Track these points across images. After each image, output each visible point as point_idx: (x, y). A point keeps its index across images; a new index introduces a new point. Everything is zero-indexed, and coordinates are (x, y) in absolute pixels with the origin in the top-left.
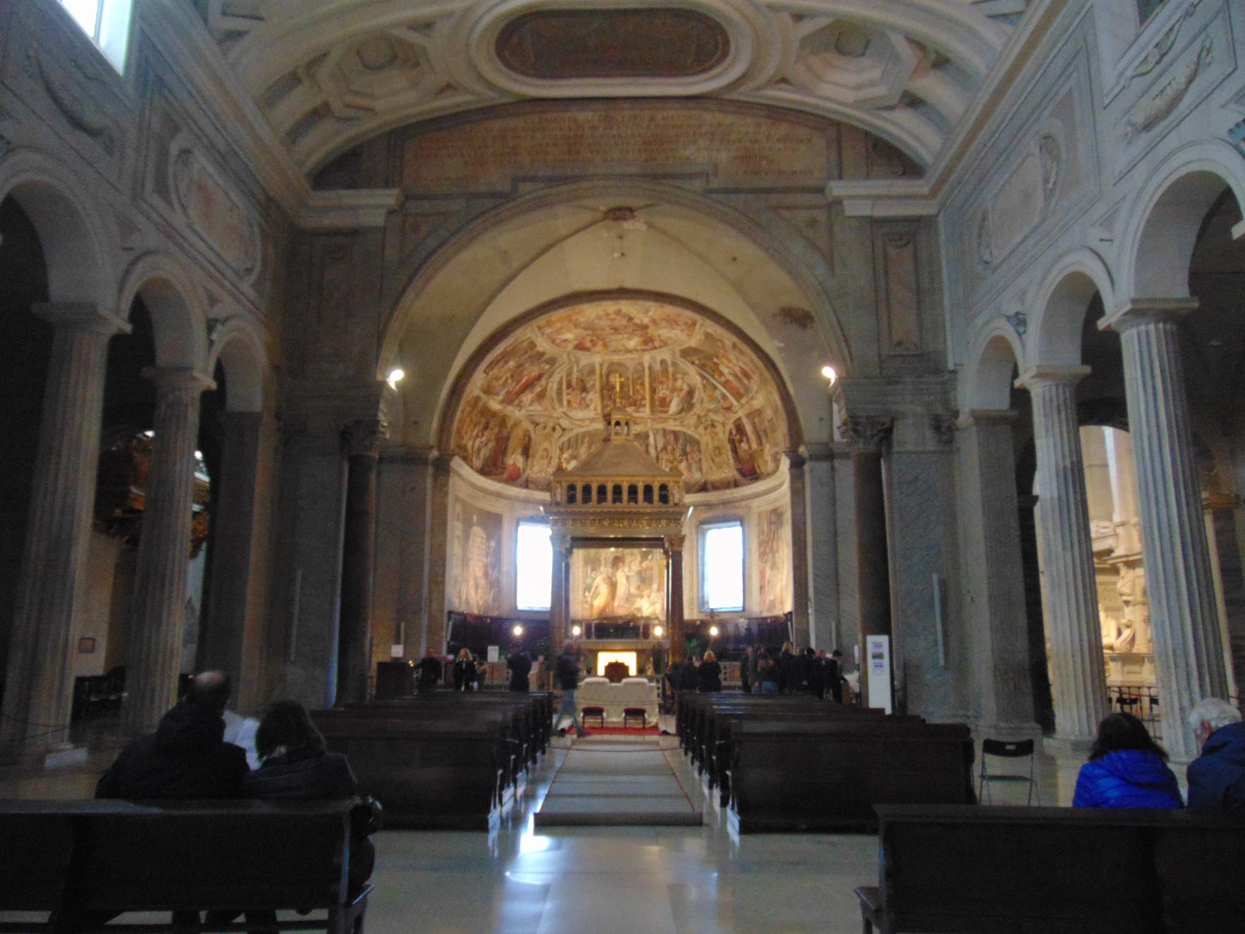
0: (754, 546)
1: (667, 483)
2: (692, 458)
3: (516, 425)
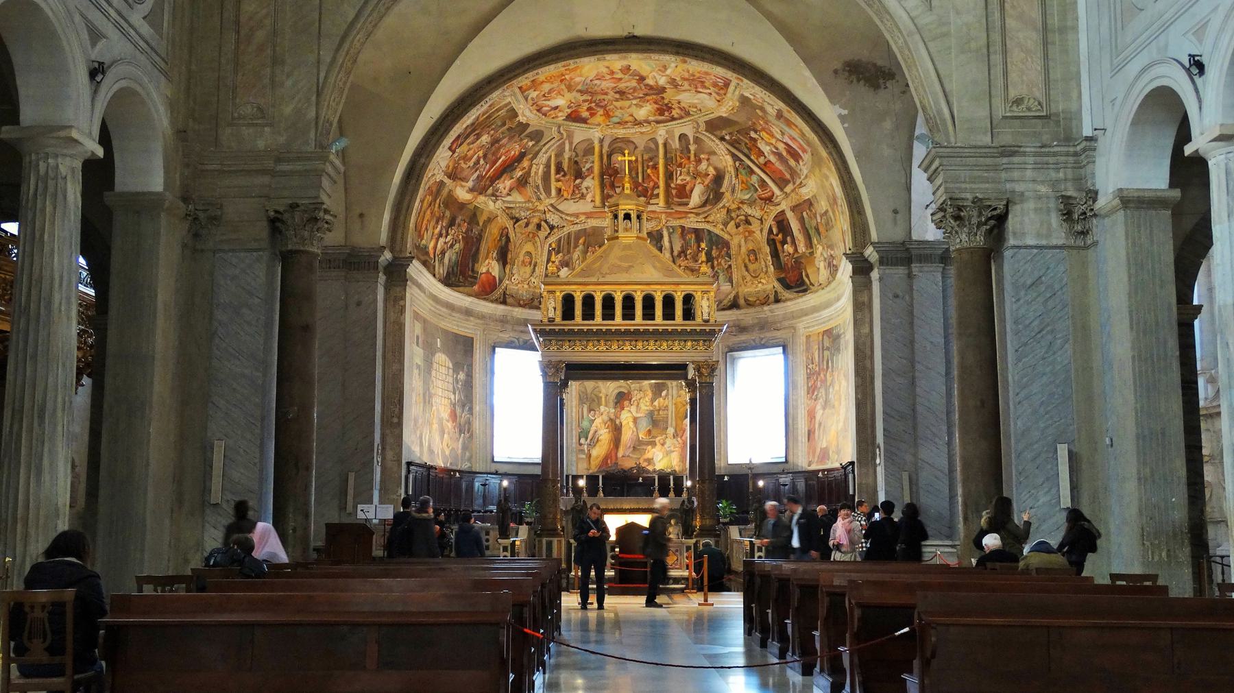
0: (801, 378)
1: (694, 293)
2: (719, 264)
3: (489, 220)
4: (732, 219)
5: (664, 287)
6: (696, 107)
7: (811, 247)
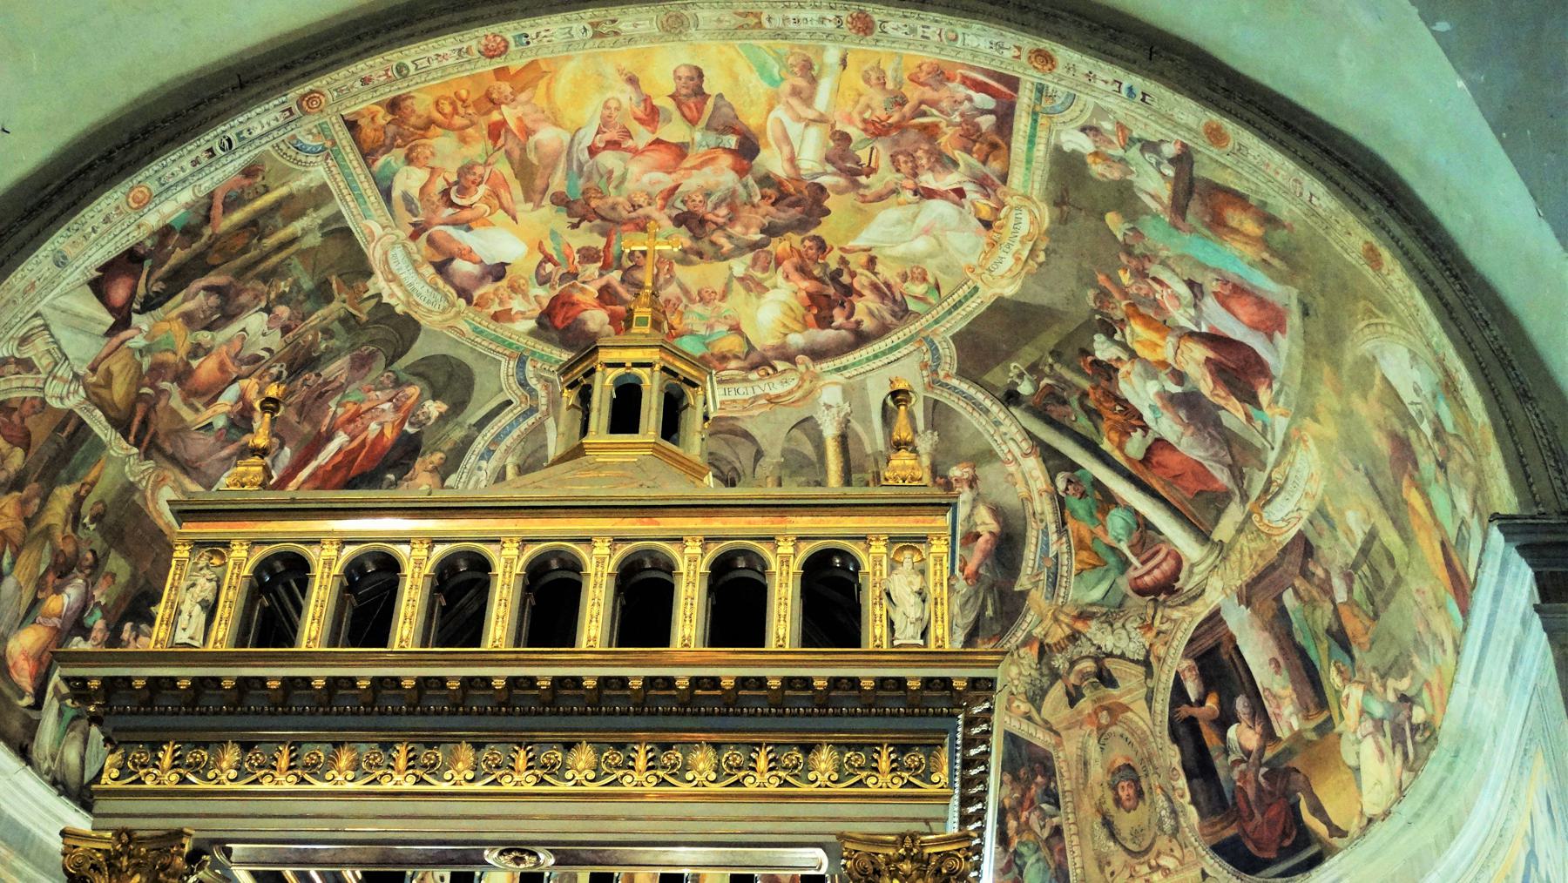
1: (856, 549)
2: (1024, 828)
4: (1055, 675)
5: (717, 524)
6: (924, 280)
7: (1322, 704)
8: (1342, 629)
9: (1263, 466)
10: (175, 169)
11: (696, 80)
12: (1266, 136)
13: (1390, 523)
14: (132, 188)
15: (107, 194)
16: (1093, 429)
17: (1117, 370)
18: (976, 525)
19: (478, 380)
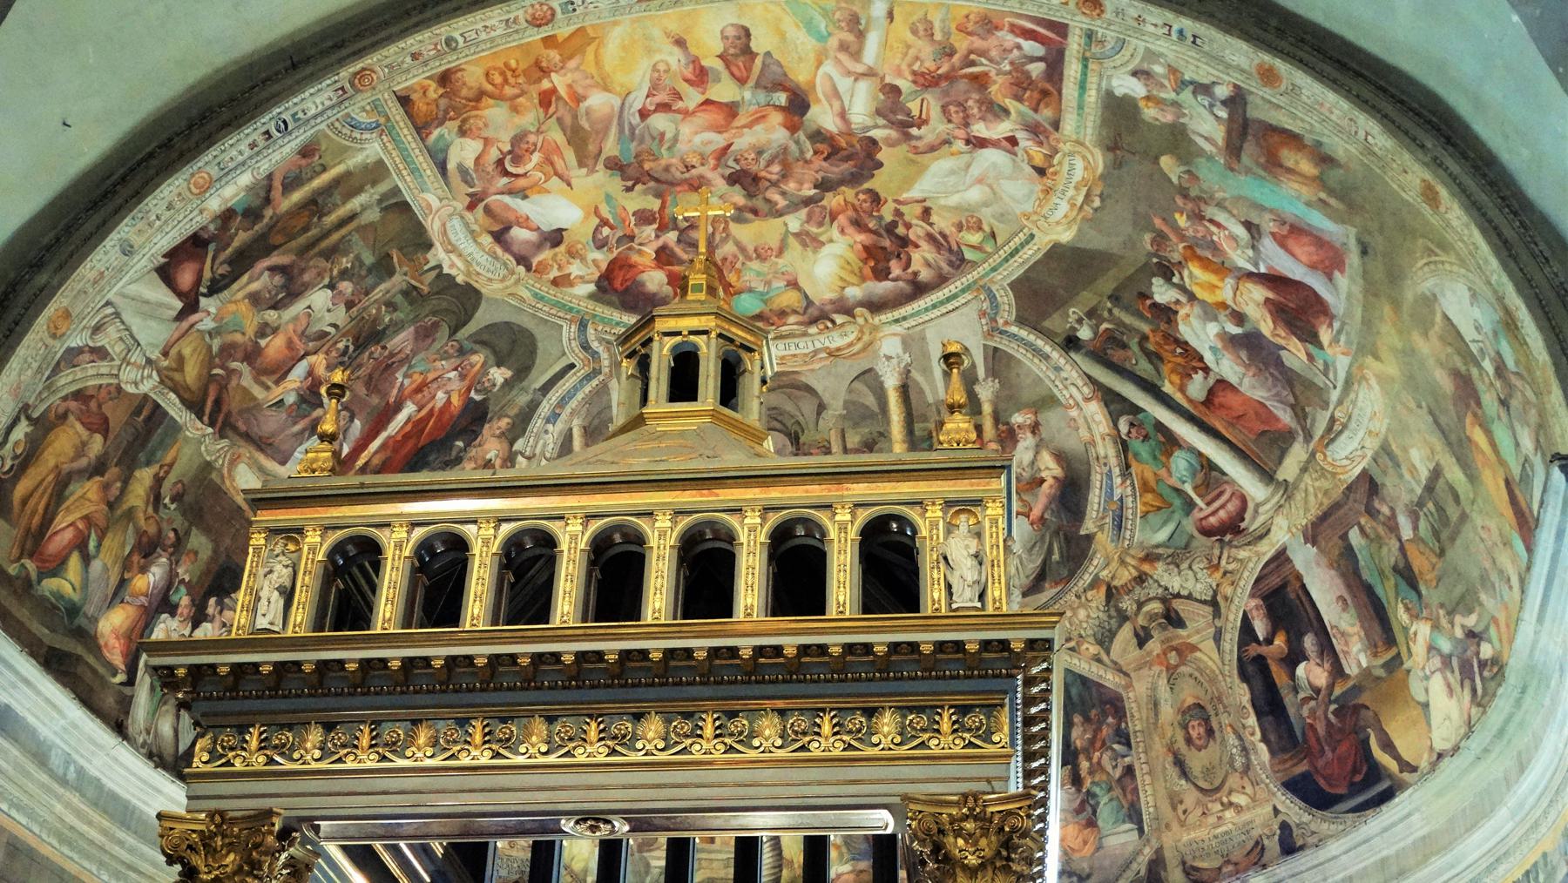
2: (1097, 768)
4: (1123, 618)
6: (980, 229)
7: (1390, 641)
8: (1408, 567)
9: (1325, 405)
10: (235, 153)
11: (744, 39)
12: (1320, 76)
13: (1454, 460)
14: (193, 175)
15: (169, 181)
16: (1154, 372)
17: (1177, 312)
18: (1040, 470)
19: (540, 345)
